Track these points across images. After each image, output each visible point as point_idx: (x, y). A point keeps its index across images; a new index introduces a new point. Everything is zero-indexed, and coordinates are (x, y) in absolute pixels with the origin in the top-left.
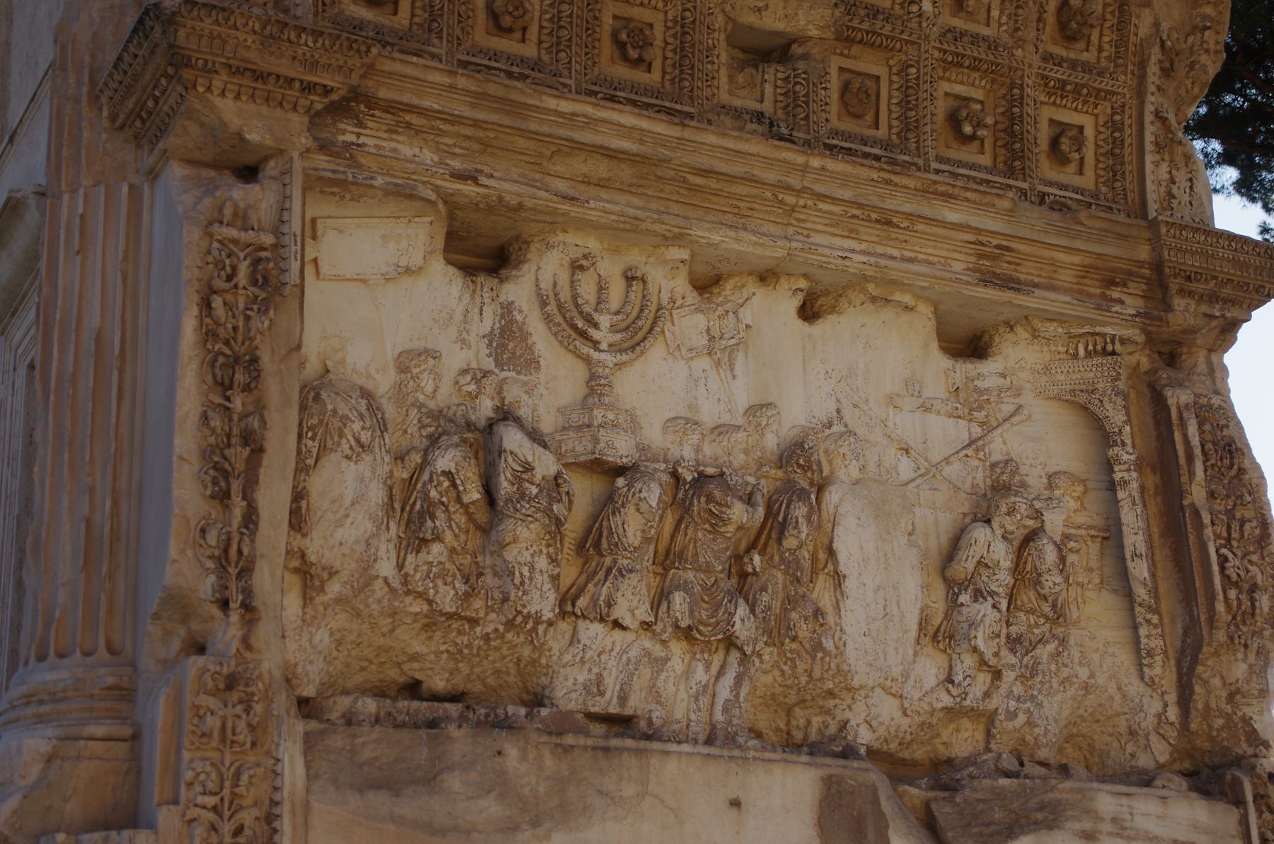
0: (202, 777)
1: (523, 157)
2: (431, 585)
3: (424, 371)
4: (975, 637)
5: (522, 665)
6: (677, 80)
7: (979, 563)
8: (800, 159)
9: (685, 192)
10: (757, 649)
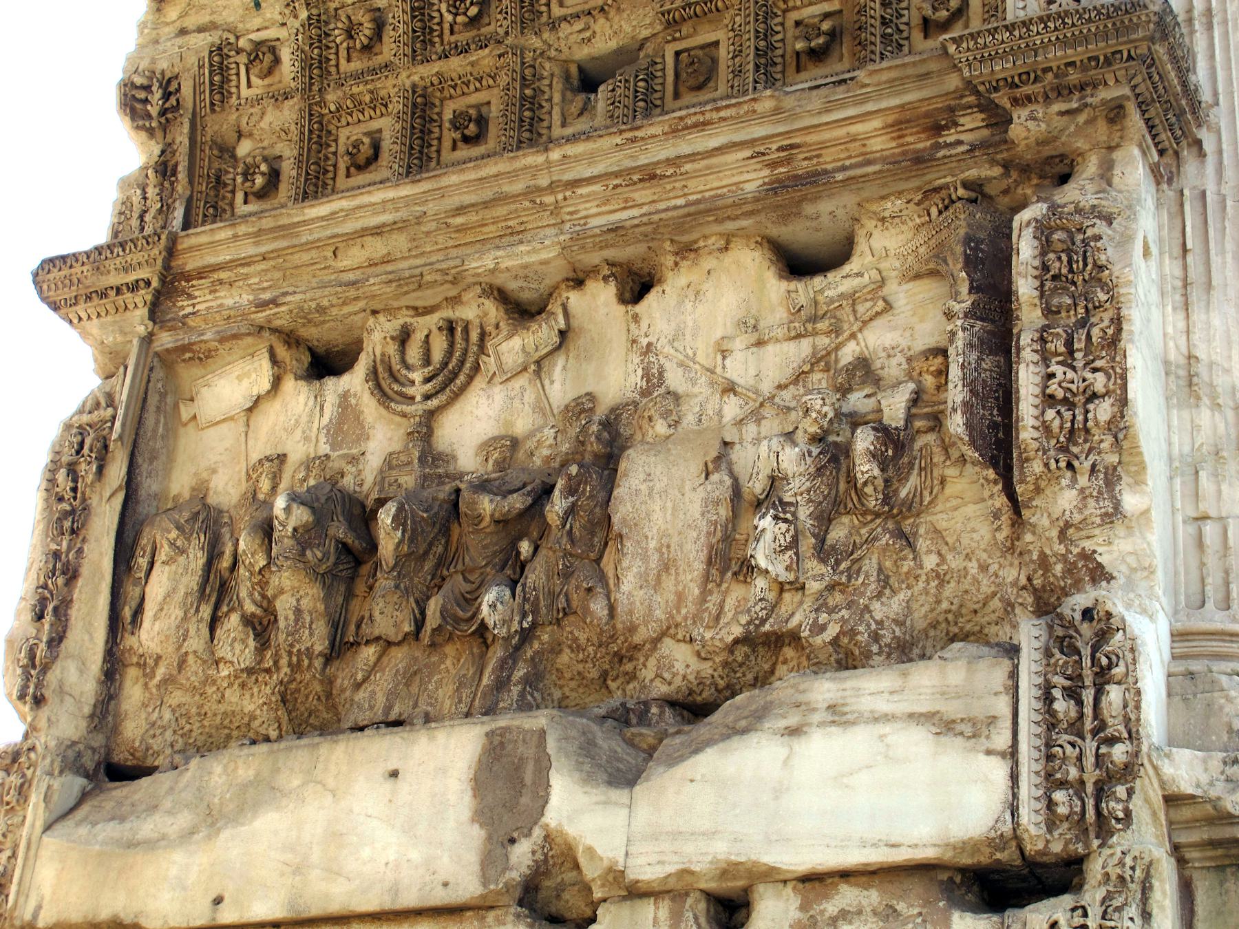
7: (773, 479)
8: (540, 159)
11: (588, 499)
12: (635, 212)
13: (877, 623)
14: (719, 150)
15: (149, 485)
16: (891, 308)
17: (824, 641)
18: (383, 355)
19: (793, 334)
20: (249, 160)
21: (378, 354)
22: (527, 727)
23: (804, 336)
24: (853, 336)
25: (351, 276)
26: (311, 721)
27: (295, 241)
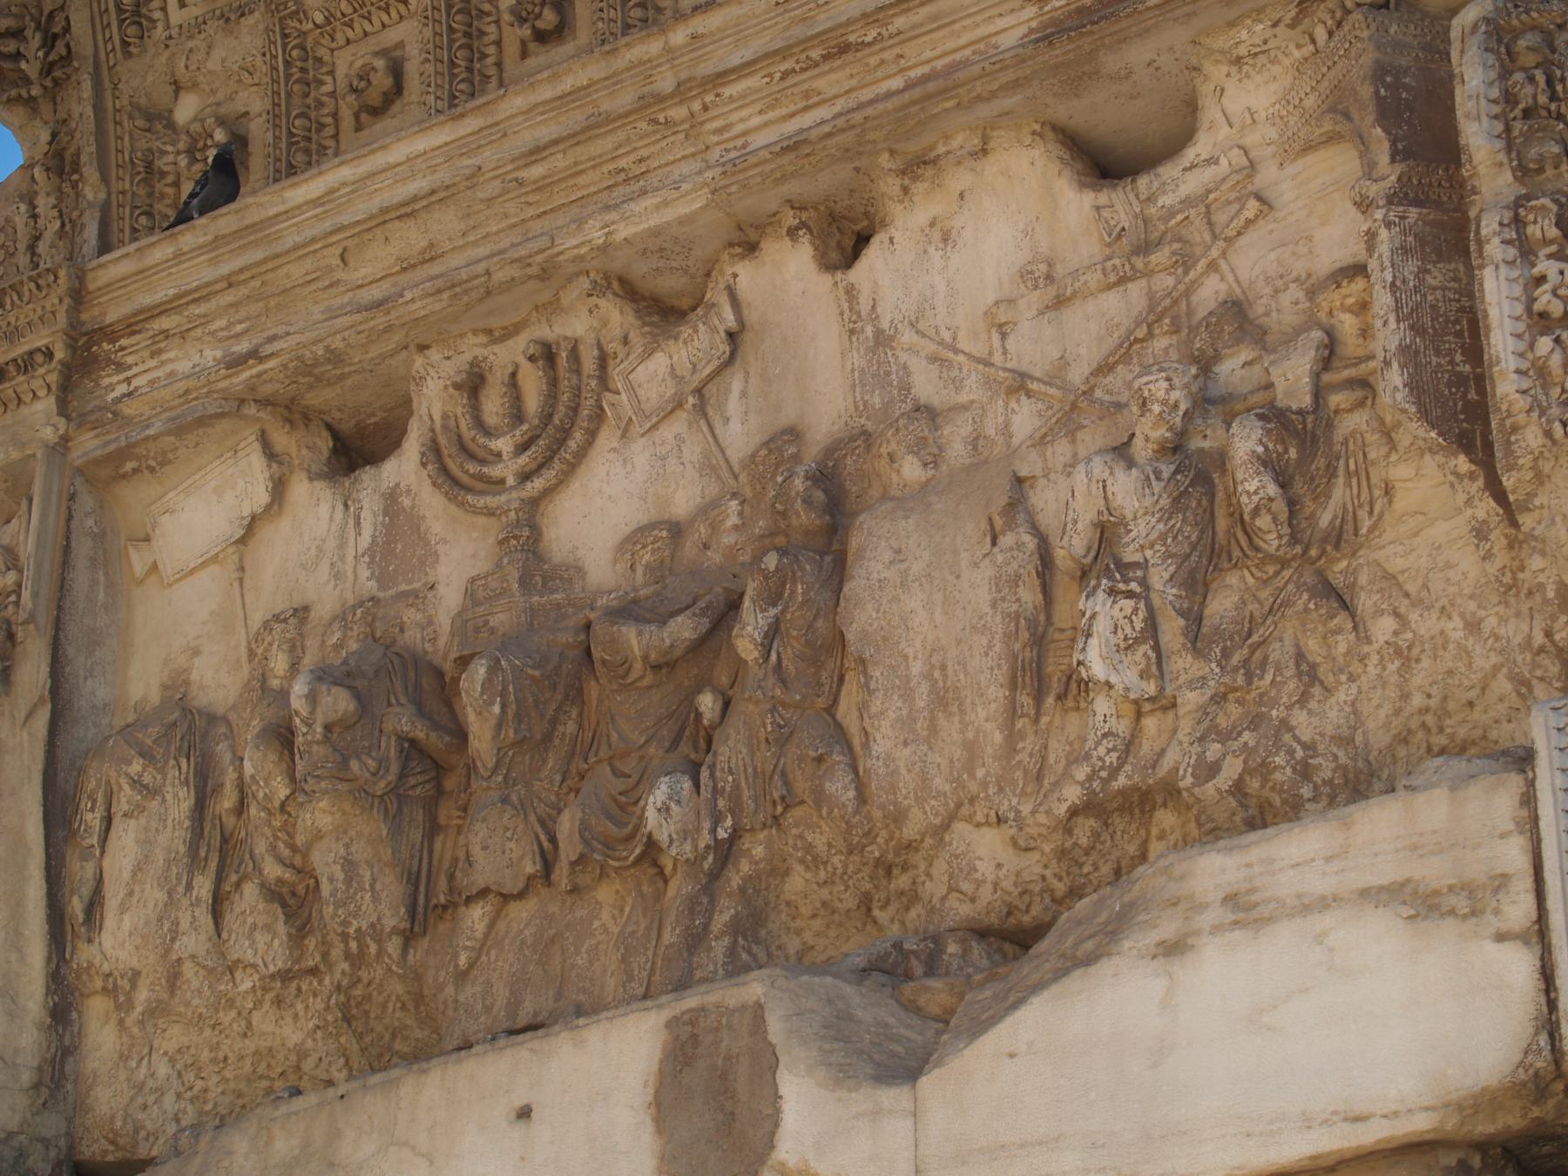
1: (314, 287)
3: (270, 644)
8: (654, 47)
10: (702, 845)
11: (803, 604)
12: (824, 113)
13: (1305, 746)
15: (92, 690)
16: (1271, 207)
17: (1219, 791)
18: (445, 417)
19: (1113, 278)
20: (195, 127)
21: (437, 417)
22: (732, 1003)
23: (1132, 279)
24: (1212, 266)
25: (374, 293)
27: (277, 248)
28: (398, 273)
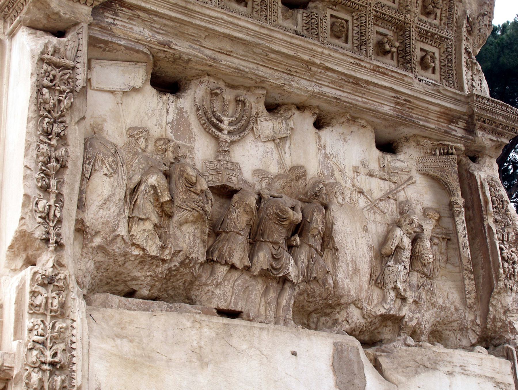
0: (36, 327)
1: (192, 37)
2: (144, 241)
3: (141, 137)
4: (396, 281)
5: (186, 285)
6: (259, 11)
7: (397, 247)
8: (320, 50)
9: (266, 61)
10: (299, 282)
14: (385, 88)
19: (383, 178)
26: (170, 292)
28: (217, 51)
